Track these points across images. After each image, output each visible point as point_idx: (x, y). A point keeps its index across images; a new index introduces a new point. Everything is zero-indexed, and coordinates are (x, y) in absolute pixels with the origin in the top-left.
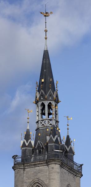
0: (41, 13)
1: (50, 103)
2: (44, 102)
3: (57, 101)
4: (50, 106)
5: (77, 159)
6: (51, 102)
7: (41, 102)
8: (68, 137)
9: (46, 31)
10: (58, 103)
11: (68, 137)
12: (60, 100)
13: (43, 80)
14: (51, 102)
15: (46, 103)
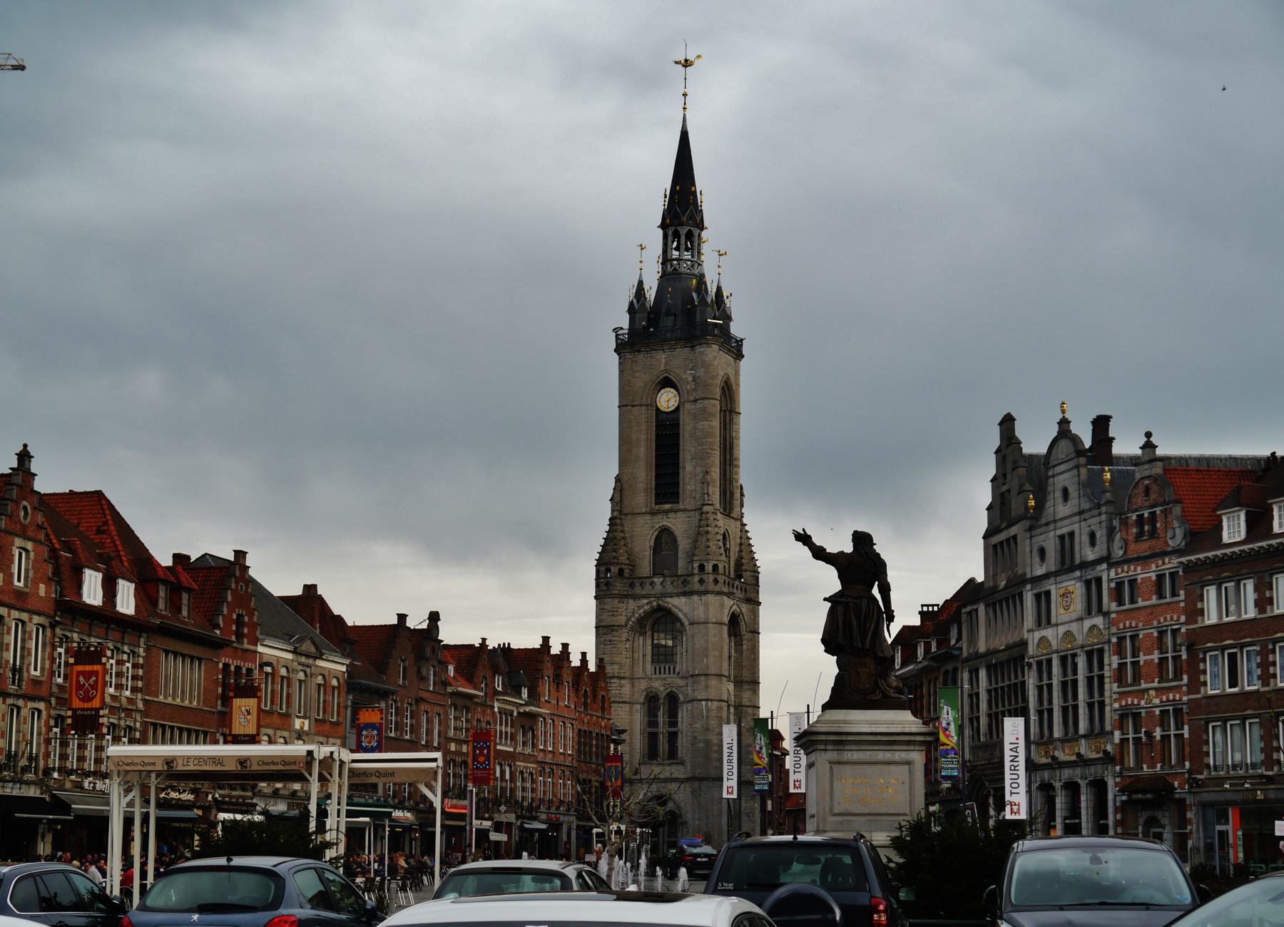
0: (676, 63)
1: (690, 230)
2: (678, 228)
3: (701, 227)
4: (689, 236)
5: (736, 329)
6: (691, 228)
7: (674, 228)
8: (719, 290)
9: (685, 95)
10: (702, 231)
11: (719, 290)
12: (706, 225)
13: (678, 188)
14: (691, 228)
15: (683, 231)
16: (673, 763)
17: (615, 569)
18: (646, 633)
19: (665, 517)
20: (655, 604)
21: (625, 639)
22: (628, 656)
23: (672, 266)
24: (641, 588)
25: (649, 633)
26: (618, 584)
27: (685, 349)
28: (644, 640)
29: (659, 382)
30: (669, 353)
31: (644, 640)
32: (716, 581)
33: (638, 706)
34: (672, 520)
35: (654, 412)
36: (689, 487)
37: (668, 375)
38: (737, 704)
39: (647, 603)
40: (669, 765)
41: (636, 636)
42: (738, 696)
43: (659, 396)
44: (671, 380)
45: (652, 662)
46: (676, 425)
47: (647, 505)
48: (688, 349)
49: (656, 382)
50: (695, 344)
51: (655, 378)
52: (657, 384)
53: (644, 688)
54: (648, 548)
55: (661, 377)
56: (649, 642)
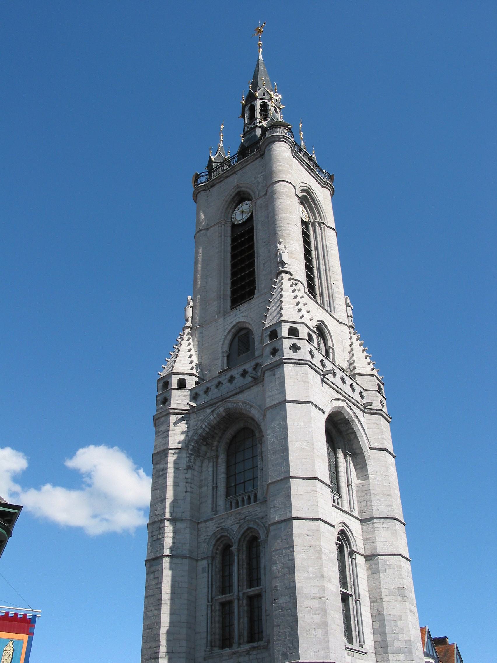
6: (266, 101)
15: (258, 102)
16: (254, 648)
17: (175, 380)
18: (217, 457)
19: (239, 312)
20: (221, 409)
21: (185, 466)
22: (189, 489)
23: (248, 127)
24: (205, 395)
25: (222, 458)
26: (177, 397)
27: (255, 162)
28: (216, 466)
29: (232, 200)
30: (241, 172)
31: (216, 466)
32: (295, 348)
33: (204, 563)
34: (245, 314)
35: (229, 229)
36: (264, 272)
37: (239, 189)
38: (369, 553)
39: (212, 412)
40: (248, 653)
41: (205, 464)
42: (368, 539)
43: (235, 212)
44: (244, 192)
45: (228, 494)
46: (251, 230)
47: (220, 312)
48: (259, 159)
49: (229, 200)
50: (263, 150)
51: (228, 197)
52: (230, 202)
53: (211, 534)
54: (220, 355)
55: (233, 195)
56: (222, 468)
